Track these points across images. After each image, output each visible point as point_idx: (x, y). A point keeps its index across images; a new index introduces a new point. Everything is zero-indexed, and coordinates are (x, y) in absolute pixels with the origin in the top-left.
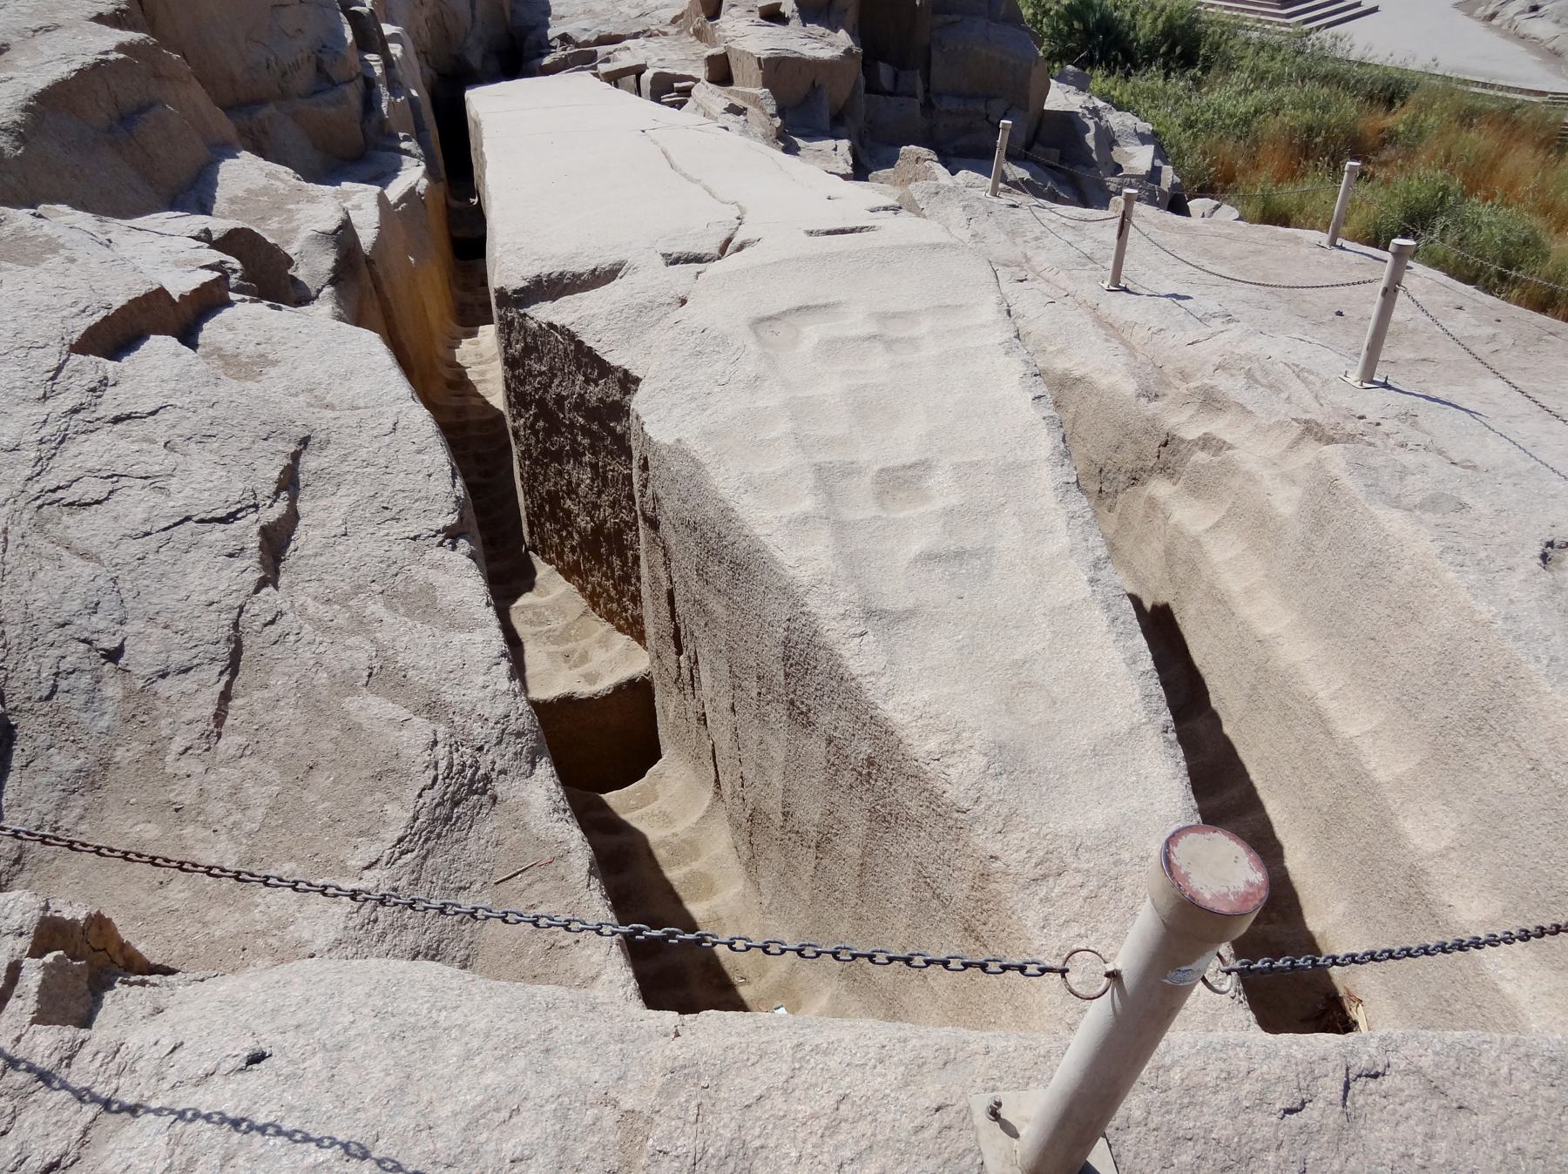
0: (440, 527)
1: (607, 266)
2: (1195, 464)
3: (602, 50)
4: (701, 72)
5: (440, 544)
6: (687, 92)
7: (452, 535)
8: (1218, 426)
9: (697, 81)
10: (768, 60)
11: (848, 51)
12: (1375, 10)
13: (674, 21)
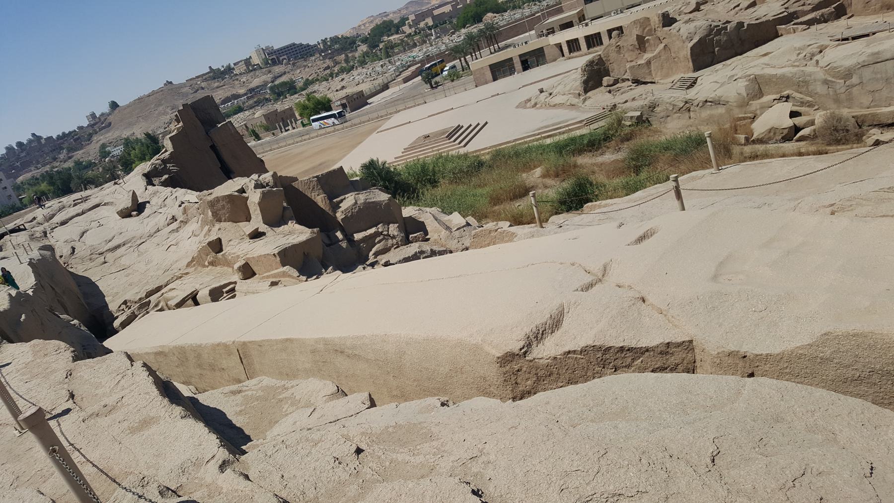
1: (555, 312)
3: (153, 299)
4: (236, 277)
6: (233, 290)
9: (235, 283)
10: (279, 253)
11: (312, 232)
12: (486, 123)
13: (188, 265)
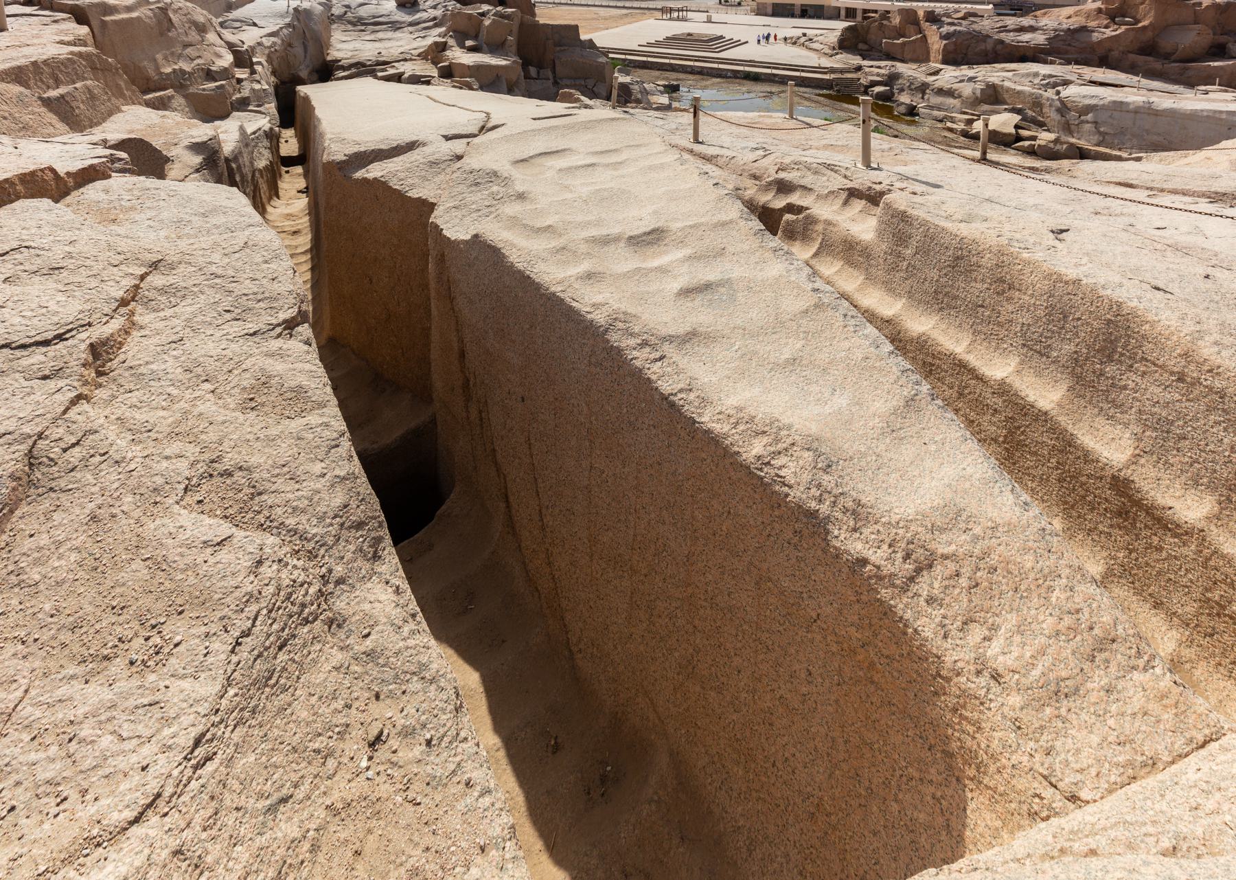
0: (281, 320)
2: (787, 222)
5: (279, 335)
7: (290, 326)
8: (795, 199)
